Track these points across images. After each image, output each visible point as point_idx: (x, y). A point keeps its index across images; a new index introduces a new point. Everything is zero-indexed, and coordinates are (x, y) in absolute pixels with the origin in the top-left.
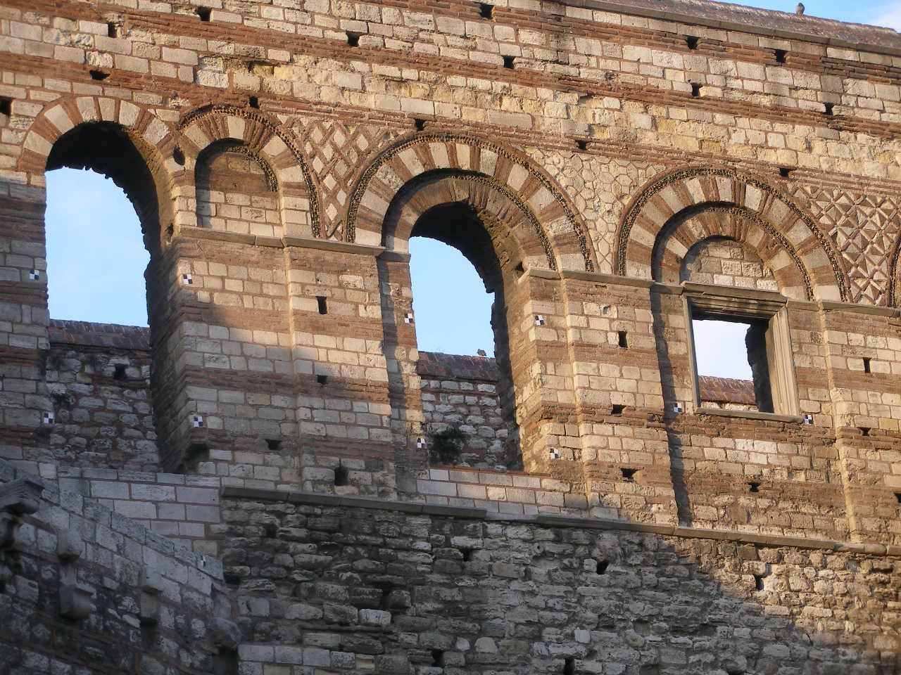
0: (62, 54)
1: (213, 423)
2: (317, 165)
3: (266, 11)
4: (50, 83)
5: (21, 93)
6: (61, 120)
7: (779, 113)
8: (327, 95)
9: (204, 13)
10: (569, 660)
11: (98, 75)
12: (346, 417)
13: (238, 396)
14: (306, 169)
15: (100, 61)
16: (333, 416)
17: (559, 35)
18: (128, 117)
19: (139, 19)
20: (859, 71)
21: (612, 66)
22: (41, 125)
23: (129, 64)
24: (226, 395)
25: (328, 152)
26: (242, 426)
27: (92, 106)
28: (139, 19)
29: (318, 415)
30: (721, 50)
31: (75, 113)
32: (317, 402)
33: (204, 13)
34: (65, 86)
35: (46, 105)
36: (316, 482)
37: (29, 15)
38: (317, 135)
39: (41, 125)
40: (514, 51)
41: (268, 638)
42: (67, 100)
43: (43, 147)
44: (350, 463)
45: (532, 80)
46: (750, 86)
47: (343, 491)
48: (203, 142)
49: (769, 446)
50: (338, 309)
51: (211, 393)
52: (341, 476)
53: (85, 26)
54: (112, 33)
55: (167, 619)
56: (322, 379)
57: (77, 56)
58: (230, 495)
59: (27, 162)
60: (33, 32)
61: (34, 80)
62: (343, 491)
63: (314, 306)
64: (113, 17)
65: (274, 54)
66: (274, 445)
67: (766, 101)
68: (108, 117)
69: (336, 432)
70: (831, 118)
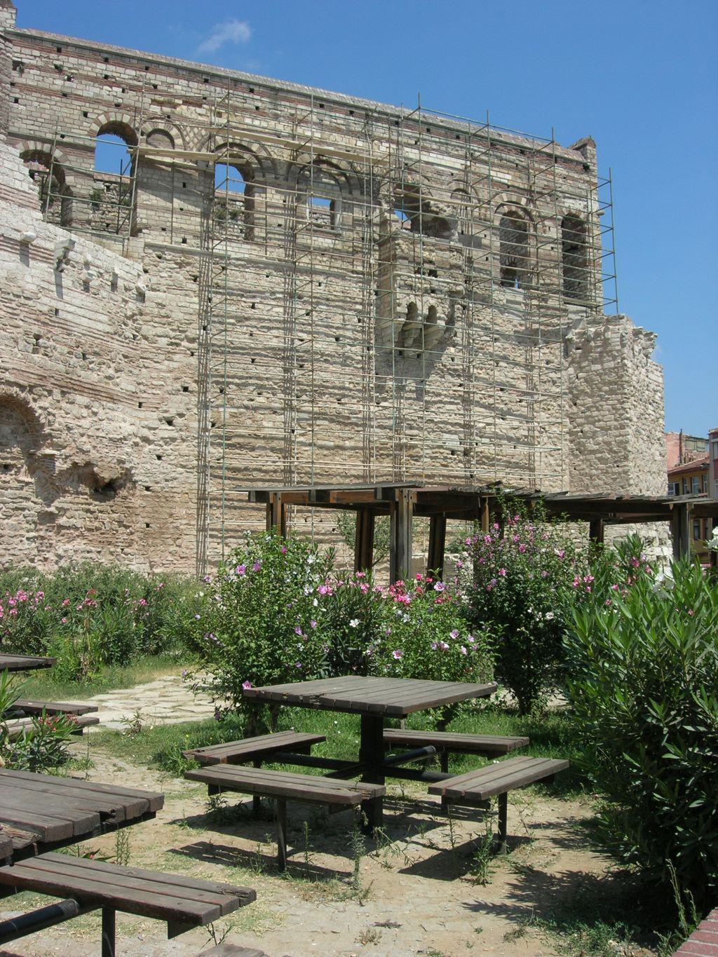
0: (106, 98)
1: (144, 221)
2: (187, 139)
3: (176, 87)
4: (101, 107)
5: (91, 110)
6: (103, 120)
7: (350, 133)
8: (194, 116)
9: (155, 87)
10: (254, 304)
11: (118, 106)
12: (188, 222)
13: (153, 213)
14: (184, 140)
15: (120, 101)
16: (183, 221)
17: (276, 99)
18: (126, 119)
19: (132, 88)
20: (378, 120)
21: (293, 112)
22: (97, 122)
23: (126, 102)
24: (149, 212)
25: (192, 135)
26: (154, 223)
27: (115, 116)
28: (132, 88)
29: (179, 221)
30: (331, 110)
31: (108, 118)
32: (179, 216)
33: (155, 87)
34: (106, 109)
35: (99, 115)
36: (176, 242)
37: (96, 85)
38: (188, 129)
39: (97, 122)
40: (259, 104)
41: (154, 290)
42: (106, 113)
43: (97, 128)
44: (187, 237)
45: (264, 114)
46: (339, 121)
47: (184, 246)
48: (150, 129)
49: (330, 241)
50: (189, 187)
51: (145, 211)
52: (184, 241)
53: (115, 89)
54: (123, 91)
55: (120, 283)
56: (182, 209)
57: (111, 98)
58: (148, 246)
59: (91, 133)
60: (97, 90)
61: (96, 106)
62: (184, 246)
63: (182, 185)
64: (124, 86)
65: (177, 101)
66: (164, 230)
67: (344, 128)
68: (119, 119)
69: (183, 226)
70: (367, 136)
